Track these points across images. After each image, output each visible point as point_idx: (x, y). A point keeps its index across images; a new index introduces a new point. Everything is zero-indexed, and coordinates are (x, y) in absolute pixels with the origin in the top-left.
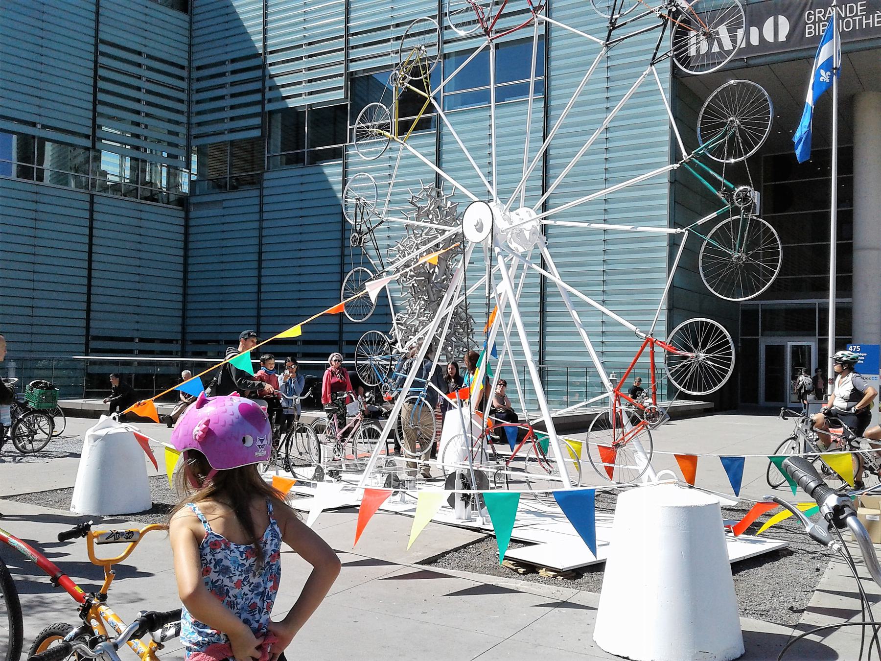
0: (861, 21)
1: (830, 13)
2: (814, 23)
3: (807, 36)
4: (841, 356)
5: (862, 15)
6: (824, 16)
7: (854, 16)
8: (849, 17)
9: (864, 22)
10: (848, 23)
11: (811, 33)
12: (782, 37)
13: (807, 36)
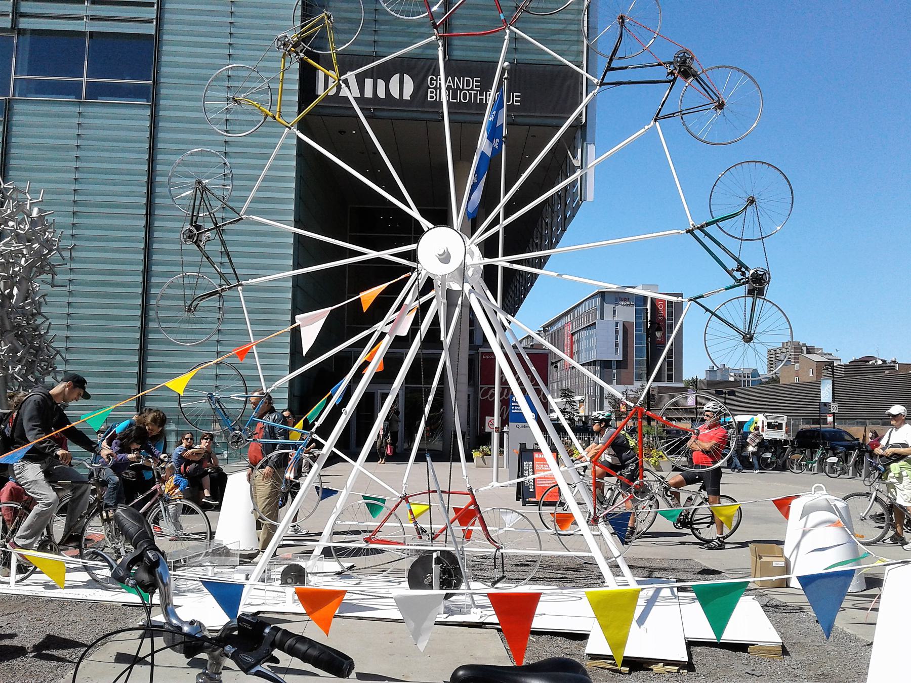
0: (476, 95)
1: (450, 82)
2: (435, 88)
3: (429, 99)
4: (598, 416)
5: (477, 91)
7: (470, 90)
8: (466, 90)
9: (479, 97)
10: (465, 94)
12: (407, 96)
13: (429, 99)
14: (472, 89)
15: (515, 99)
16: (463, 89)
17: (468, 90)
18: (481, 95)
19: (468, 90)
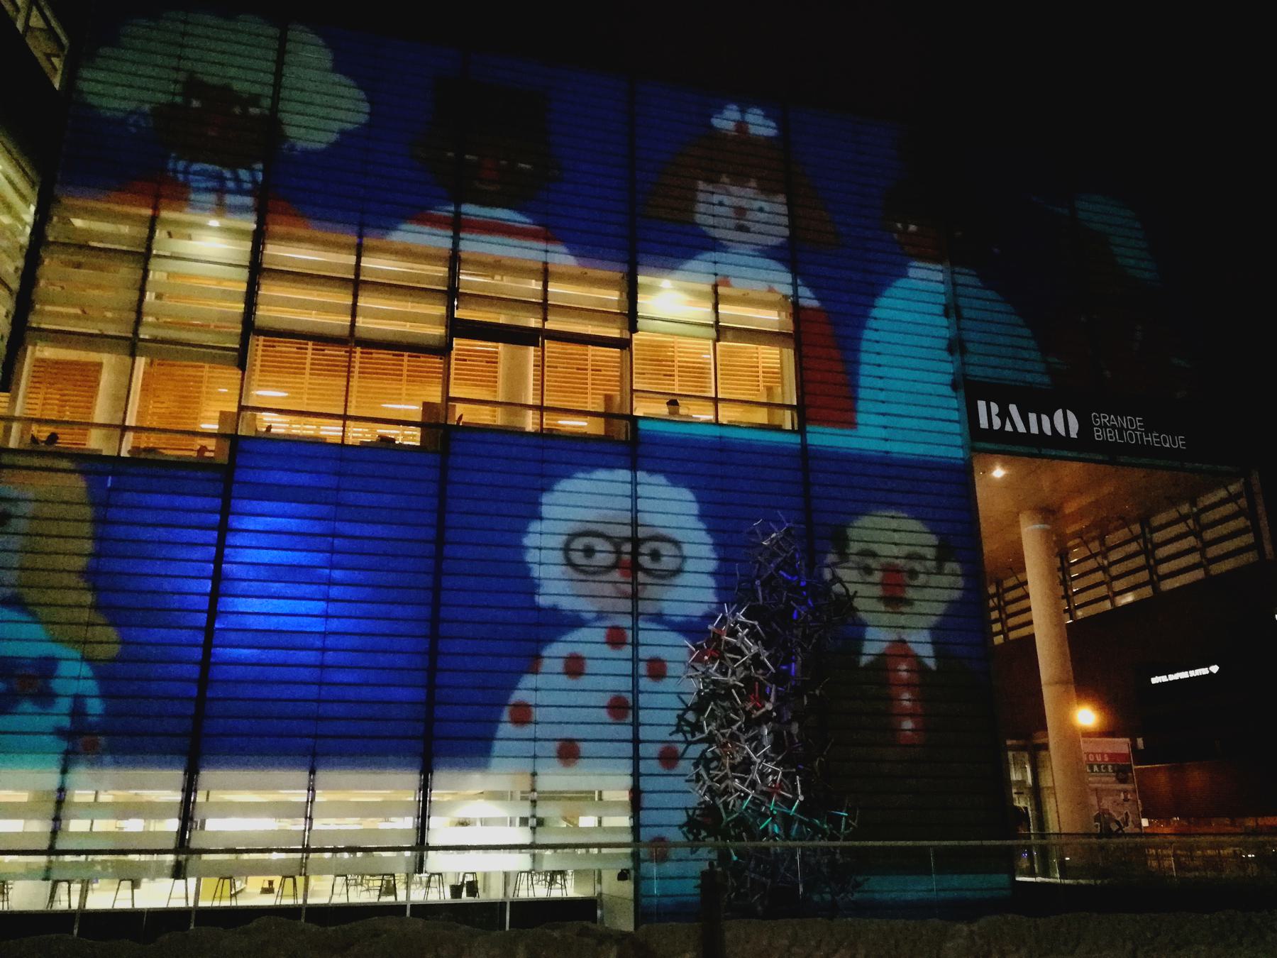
0: (1141, 435)
5: (1142, 431)
6: (1109, 421)
10: (1130, 434)
11: (1099, 436)
12: (1073, 434)
14: (1136, 430)
15: (1180, 443)
16: (1128, 429)
17: (1133, 430)
18: (1147, 436)
19: (1133, 430)
